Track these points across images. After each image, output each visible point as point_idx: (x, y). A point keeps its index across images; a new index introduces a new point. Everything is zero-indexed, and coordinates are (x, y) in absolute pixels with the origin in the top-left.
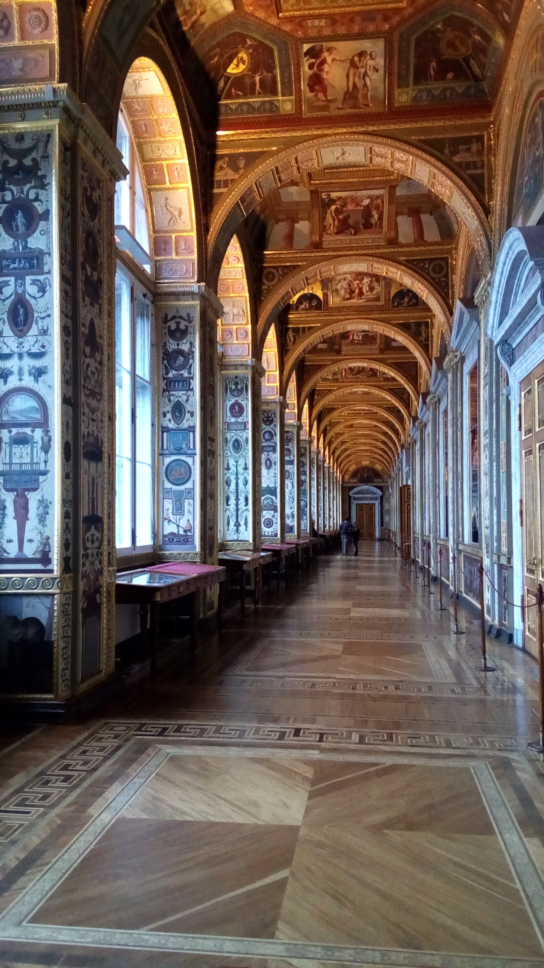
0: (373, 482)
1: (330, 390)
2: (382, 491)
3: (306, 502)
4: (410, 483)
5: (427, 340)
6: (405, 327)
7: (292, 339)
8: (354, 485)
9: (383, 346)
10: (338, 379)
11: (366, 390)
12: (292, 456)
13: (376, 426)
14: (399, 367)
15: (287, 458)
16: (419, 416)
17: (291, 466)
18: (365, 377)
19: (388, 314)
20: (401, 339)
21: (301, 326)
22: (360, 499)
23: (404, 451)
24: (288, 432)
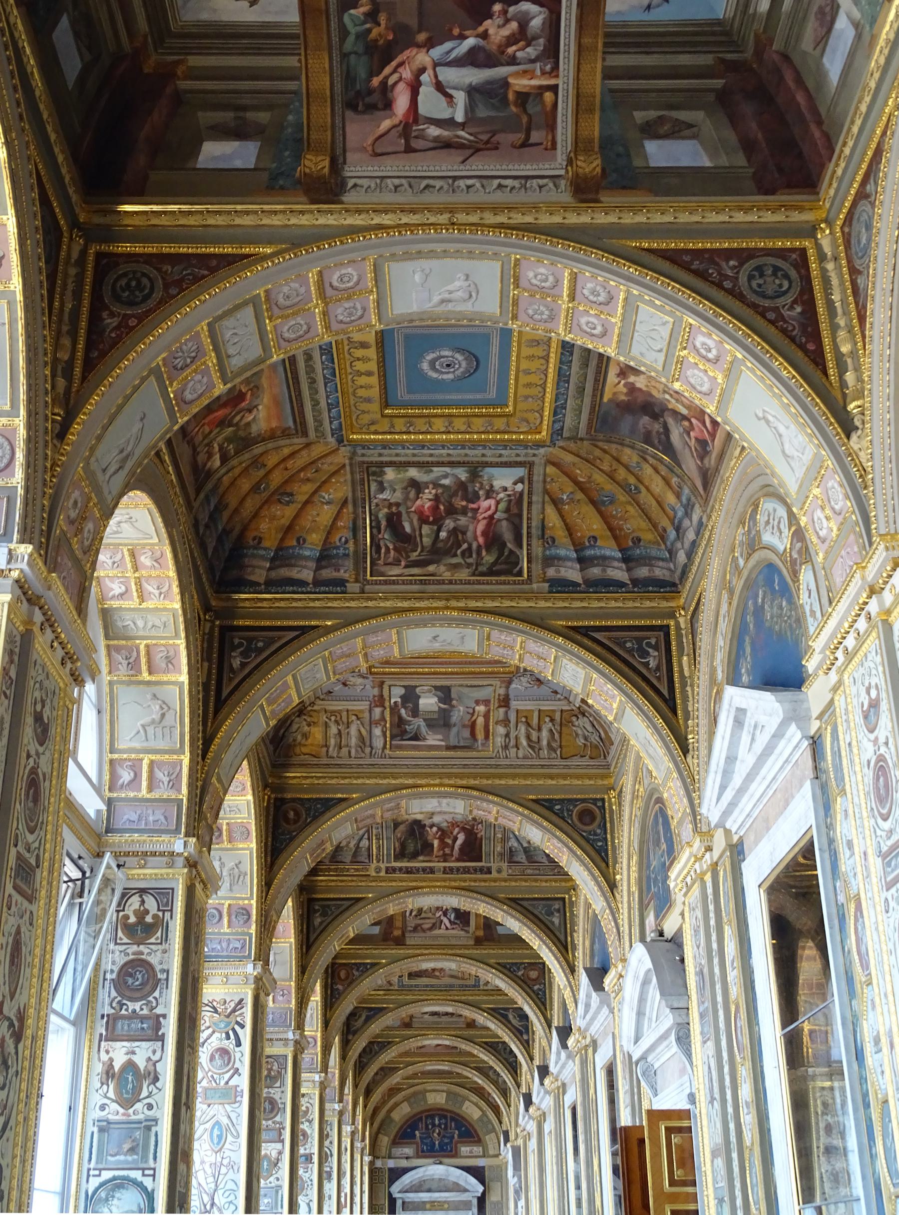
0: (455, 1154)
1: (304, 630)
2: (483, 1182)
3: (150, 1197)
8: (404, 1163)
9: (591, 166)
10: (342, 583)
18: (463, 574)
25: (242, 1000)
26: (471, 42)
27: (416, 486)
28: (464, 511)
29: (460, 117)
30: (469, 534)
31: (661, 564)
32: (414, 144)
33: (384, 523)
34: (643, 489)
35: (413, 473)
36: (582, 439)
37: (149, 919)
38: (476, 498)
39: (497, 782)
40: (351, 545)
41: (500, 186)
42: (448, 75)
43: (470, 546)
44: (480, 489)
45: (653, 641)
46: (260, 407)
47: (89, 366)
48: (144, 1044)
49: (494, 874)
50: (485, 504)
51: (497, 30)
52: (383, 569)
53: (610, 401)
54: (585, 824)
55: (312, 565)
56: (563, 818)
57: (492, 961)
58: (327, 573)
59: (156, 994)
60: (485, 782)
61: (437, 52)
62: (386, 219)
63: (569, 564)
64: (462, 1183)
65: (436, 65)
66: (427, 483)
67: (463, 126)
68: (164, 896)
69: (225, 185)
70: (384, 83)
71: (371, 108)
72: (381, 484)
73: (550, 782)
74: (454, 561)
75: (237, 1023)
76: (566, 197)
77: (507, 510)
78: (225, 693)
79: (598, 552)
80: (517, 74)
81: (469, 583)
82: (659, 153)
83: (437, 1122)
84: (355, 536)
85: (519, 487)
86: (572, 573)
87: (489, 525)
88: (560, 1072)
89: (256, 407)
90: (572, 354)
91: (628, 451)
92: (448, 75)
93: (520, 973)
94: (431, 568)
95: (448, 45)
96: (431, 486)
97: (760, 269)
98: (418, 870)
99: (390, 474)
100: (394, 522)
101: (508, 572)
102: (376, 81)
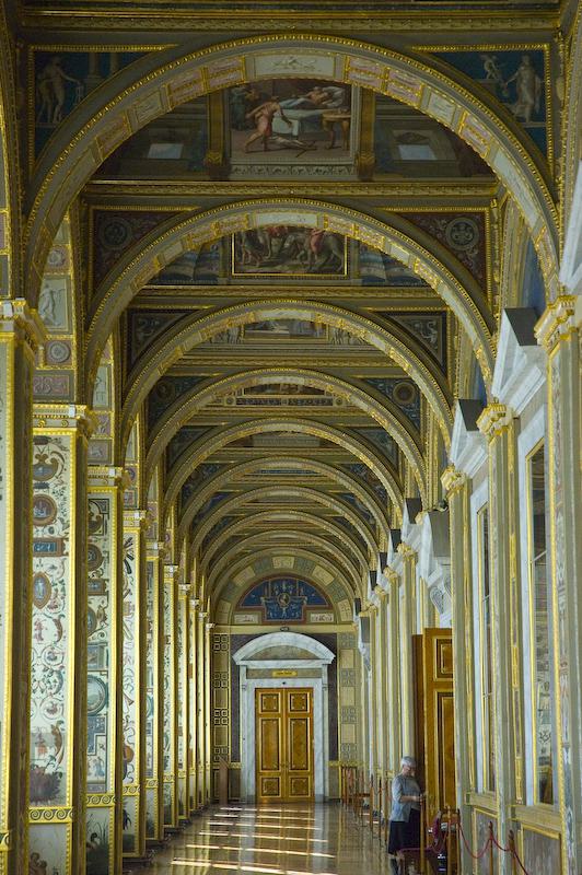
0: (305, 622)
1: (188, 312)
2: (333, 649)
3: (106, 687)
4: (445, 620)
5: (538, 116)
6: (462, 68)
7: (61, 97)
9: (368, 159)
10: (214, 277)
11: (306, 315)
12: (58, 526)
13: (325, 443)
14: (421, 227)
15: (39, 533)
16: (495, 390)
17: (56, 561)
19: (402, 20)
20: (445, 106)
21: (94, 49)
22: (267, 674)
23: (424, 519)
24: (44, 440)
25: (131, 539)
26: (301, 100)
29: (295, 133)
32: (269, 146)
37: (94, 519)
39: (332, 364)
40: (221, 252)
41: (317, 170)
42: (288, 113)
43: (306, 252)
45: (434, 323)
47: (96, 283)
48: (96, 598)
49: (335, 405)
51: (316, 95)
52: (244, 268)
54: (404, 399)
55: (193, 264)
56: (385, 394)
57: (336, 463)
58: (204, 271)
59: (102, 566)
60: (322, 364)
61: (283, 104)
62: (253, 192)
63: (377, 265)
64: (311, 650)
65: (282, 109)
67: (297, 137)
68: (103, 504)
69: (165, 169)
70: (253, 117)
71: (246, 128)
73: (375, 364)
74: (295, 262)
75: (128, 556)
76: (355, 178)
78: (134, 359)
80: (327, 113)
81: (306, 278)
82: (408, 153)
83: (284, 588)
84: (224, 247)
86: (380, 272)
88: (395, 568)
92: (288, 113)
93: (363, 474)
94: (278, 268)
95: (289, 101)
97: (457, 226)
98: (266, 401)
101: (333, 271)
102: (248, 116)
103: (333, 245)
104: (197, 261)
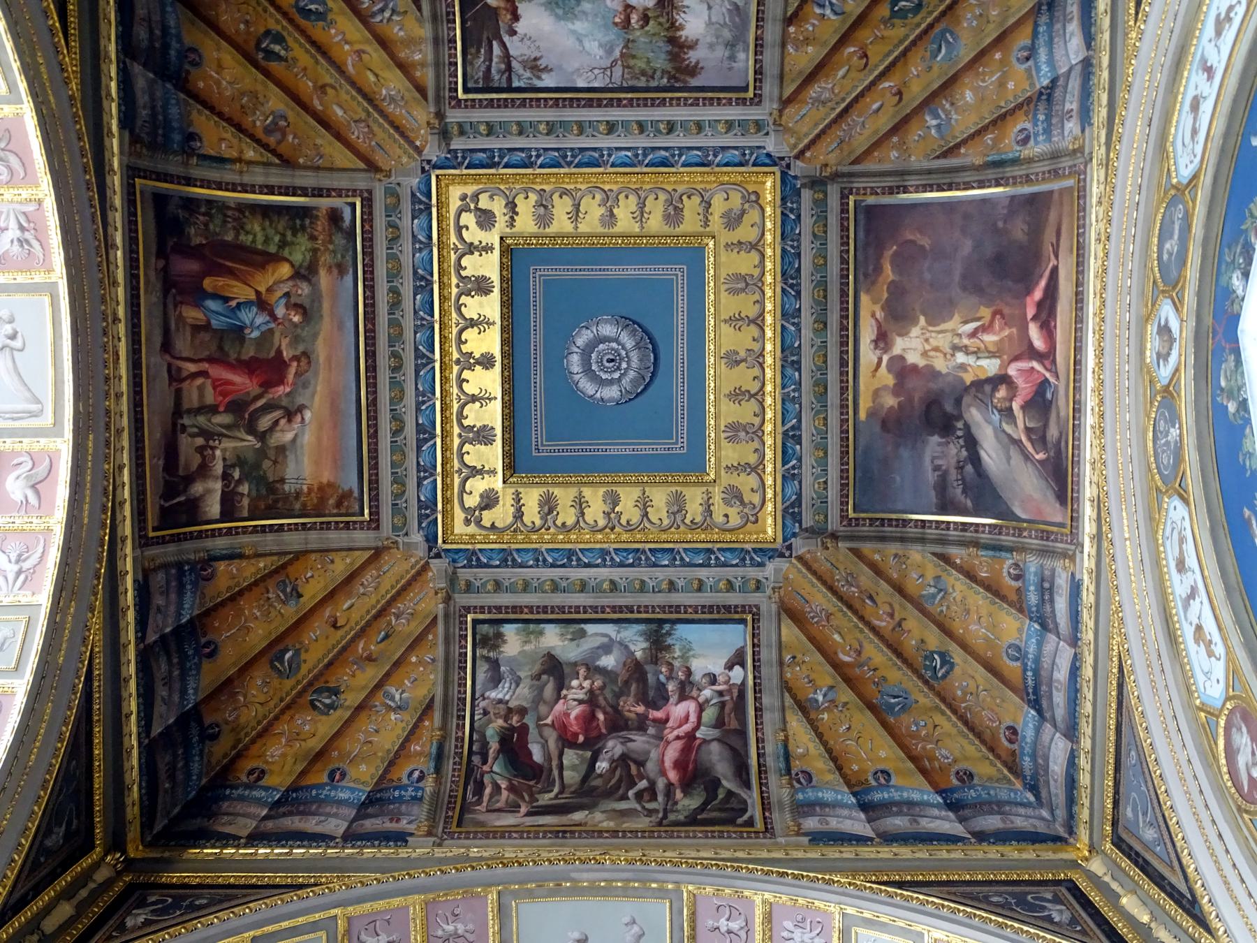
27: (554, 669)
28: (641, 724)
30: (651, 767)
31: (1022, 811)
33: (494, 745)
34: (957, 655)
35: (552, 638)
36: (834, 536)
38: (659, 698)
43: (652, 784)
44: (669, 678)
46: (308, 415)
50: (679, 710)
53: (872, 414)
63: (846, 812)
66: (575, 664)
72: (495, 664)
74: (623, 805)
77: (719, 723)
79: (896, 796)
85: (737, 674)
87: (686, 750)
89: (300, 409)
90: (798, 294)
91: (916, 554)
94: (578, 816)
96: (582, 671)
99: (513, 642)
100: (513, 745)
103: (717, 759)
104: (364, 805)
